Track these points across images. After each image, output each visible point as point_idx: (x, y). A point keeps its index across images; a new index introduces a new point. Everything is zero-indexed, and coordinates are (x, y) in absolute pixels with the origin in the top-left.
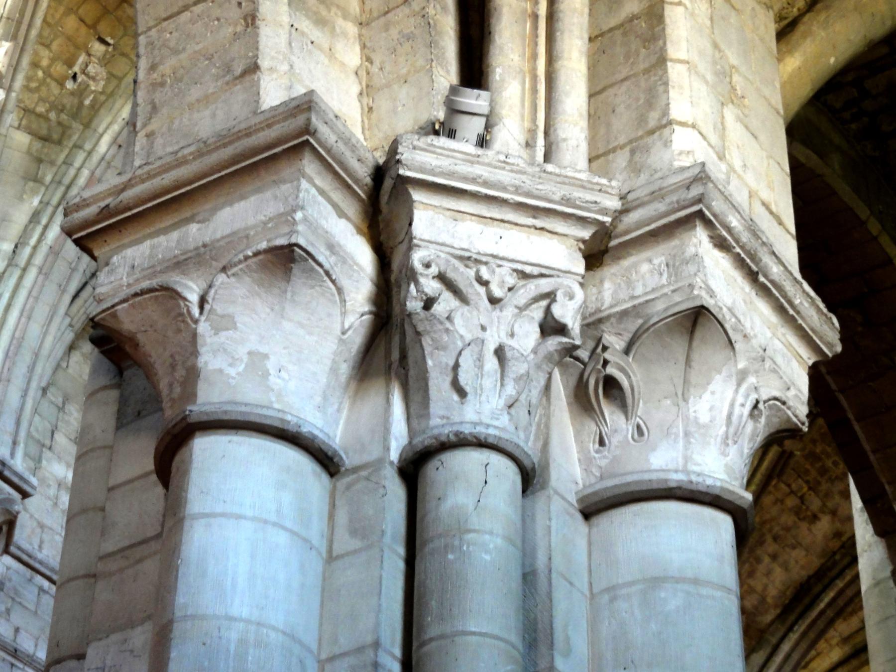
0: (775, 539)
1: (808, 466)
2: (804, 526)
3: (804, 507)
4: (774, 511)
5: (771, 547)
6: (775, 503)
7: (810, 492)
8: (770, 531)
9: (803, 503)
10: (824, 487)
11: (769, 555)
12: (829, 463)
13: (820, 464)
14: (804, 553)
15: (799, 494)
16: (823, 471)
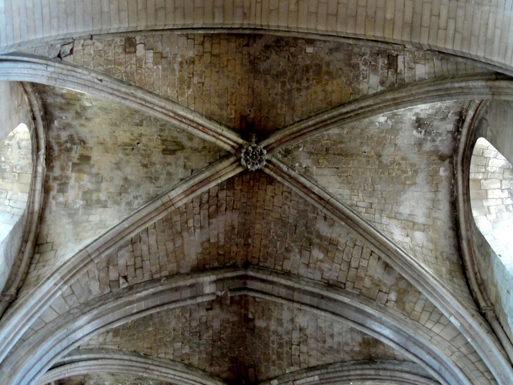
0: (324, 342)
1: (285, 355)
2: (308, 332)
3: (301, 340)
4: (314, 353)
5: (329, 342)
6: (309, 356)
7: (293, 343)
8: (323, 348)
9: (300, 342)
10: (286, 338)
11: (333, 339)
12: (275, 346)
13: (279, 350)
14: (319, 320)
15: (298, 347)
16: (281, 345)
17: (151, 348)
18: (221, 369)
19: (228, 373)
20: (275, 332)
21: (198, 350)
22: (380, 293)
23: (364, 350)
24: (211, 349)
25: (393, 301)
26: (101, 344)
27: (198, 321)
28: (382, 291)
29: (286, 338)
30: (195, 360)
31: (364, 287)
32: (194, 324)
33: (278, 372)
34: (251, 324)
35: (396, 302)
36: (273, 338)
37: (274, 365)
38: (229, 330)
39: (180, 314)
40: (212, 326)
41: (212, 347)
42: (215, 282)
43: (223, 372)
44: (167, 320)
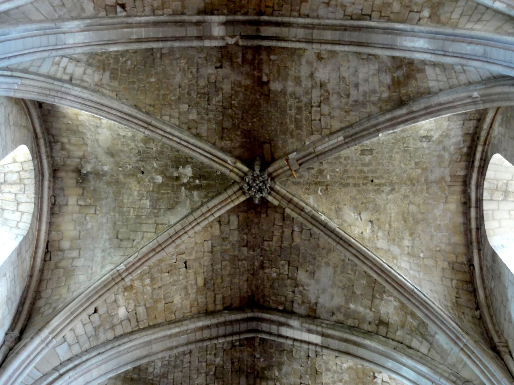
0: (348, 96)
1: (304, 122)
3: (322, 98)
4: (336, 113)
6: (332, 118)
7: (313, 104)
8: (347, 104)
9: (321, 102)
11: (358, 90)
12: (293, 112)
13: (298, 117)
14: (342, 69)
15: (319, 109)
16: (299, 110)
17: (154, 106)
18: (233, 144)
19: (242, 150)
20: (293, 95)
21: (206, 117)
22: (412, 13)
23: (394, 94)
24: (221, 118)
25: (426, 18)
26: (97, 85)
27: (206, 80)
28: (413, 11)
29: (305, 100)
30: (203, 130)
31: (392, 13)
32: (202, 82)
33: (297, 145)
34: (266, 88)
35: (430, 17)
36: (291, 102)
37: (292, 136)
38: (241, 96)
39: (186, 67)
40: (222, 89)
41: (223, 116)
42: (226, 24)
43: (235, 148)
44: (172, 72)
